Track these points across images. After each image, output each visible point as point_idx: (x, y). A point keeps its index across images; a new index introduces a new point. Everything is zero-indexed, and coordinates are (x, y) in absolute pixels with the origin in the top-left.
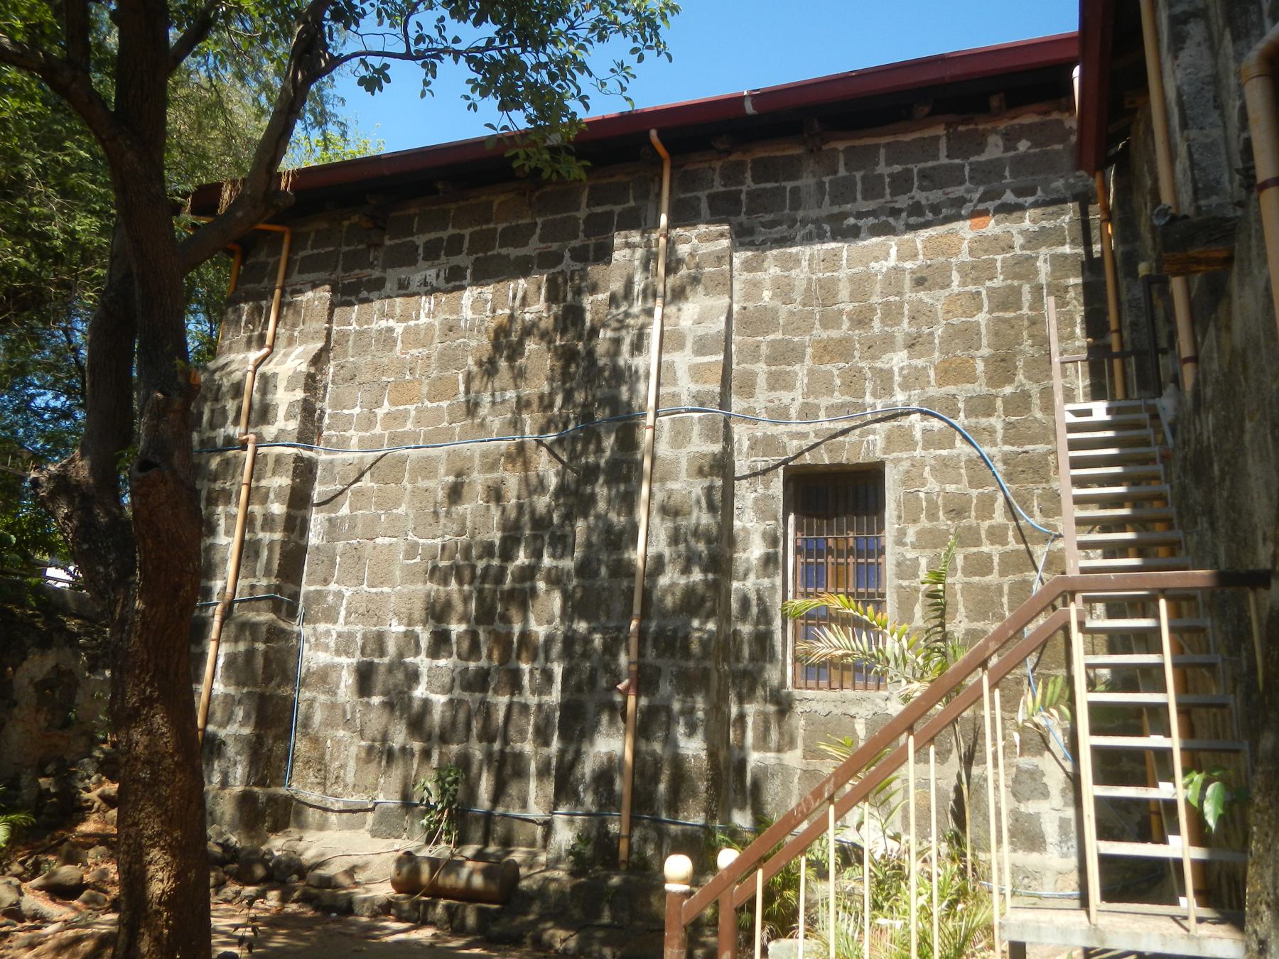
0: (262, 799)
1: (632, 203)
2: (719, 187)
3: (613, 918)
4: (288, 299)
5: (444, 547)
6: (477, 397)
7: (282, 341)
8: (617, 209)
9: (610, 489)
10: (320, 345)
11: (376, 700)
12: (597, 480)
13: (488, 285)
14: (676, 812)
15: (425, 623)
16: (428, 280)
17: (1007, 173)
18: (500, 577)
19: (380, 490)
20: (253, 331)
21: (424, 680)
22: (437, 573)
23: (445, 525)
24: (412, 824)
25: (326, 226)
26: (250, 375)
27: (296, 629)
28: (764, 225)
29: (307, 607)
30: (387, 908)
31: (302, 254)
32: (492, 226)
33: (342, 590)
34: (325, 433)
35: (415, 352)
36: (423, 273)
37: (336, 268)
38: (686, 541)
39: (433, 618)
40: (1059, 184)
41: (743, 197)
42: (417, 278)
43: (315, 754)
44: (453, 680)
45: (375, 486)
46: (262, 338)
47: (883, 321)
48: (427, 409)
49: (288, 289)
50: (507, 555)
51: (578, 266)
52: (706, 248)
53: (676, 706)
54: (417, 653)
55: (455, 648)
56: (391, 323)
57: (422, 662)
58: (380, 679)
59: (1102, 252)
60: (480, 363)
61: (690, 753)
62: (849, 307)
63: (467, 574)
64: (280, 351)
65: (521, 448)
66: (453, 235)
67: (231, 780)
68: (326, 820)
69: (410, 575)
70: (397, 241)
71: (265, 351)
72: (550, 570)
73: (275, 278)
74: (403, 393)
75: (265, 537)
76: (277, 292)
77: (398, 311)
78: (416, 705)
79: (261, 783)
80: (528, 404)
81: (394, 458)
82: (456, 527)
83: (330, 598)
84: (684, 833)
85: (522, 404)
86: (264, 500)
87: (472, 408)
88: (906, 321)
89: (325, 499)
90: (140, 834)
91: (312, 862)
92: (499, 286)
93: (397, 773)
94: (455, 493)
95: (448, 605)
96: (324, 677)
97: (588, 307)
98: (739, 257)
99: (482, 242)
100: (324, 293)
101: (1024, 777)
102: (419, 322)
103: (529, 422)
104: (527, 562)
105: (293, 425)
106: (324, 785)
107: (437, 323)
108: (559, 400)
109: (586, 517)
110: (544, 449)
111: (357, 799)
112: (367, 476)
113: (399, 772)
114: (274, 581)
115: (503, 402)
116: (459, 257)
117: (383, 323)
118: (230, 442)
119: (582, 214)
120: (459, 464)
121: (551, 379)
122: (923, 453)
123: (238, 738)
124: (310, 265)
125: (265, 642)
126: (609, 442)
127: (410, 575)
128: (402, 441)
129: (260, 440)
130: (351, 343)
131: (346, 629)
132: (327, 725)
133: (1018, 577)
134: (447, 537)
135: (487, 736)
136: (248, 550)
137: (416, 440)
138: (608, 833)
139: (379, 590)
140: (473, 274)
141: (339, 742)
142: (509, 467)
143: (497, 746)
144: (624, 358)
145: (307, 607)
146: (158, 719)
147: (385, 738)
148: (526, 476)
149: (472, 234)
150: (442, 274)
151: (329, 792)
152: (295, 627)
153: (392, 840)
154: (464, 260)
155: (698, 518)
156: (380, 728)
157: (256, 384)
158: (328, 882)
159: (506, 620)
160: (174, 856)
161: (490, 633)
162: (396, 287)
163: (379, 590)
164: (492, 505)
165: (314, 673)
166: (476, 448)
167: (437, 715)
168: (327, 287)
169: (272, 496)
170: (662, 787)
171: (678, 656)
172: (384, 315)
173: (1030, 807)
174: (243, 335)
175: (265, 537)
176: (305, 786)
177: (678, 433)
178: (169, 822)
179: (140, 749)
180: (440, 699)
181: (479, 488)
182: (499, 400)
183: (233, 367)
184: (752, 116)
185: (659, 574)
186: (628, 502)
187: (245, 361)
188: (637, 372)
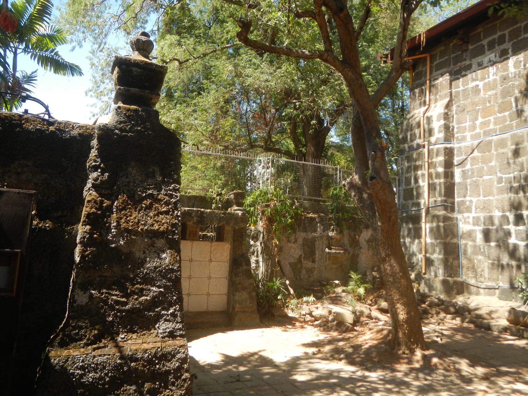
0: (451, 282)
4: (433, 83)
5: (514, 178)
6: (522, 107)
7: (433, 101)
10: (448, 99)
11: (493, 244)
13: (520, 53)
15: (510, 211)
16: (491, 59)
19: (482, 156)
20: (421, 100)
21: (513, 235)
22: (513, 190)
23: (514, 168)
24: (516, 296)
25: (443, 48)
26: (422, 118)
27: (455, 216)
29: (459, 207)
30: (505, 330)
31: (435, 63)
33: (472, 200)
34: (456, 136)
35: (489, 93)
36: (489, 57)
37: (450, 65)
43: (470, 265)
45: (480, 155)
46: (425, 102)
48: (499, 118)
49: (432, 79)
54: (509, 224)
56: (477, 83)
57: (512, 228)
58: (493, 235)
60: (521, 92)
64: (433, 105)
66: (500, 35)
67: (438, 275)
68: (479, 291)
69: (501, 191)
70: (475, 46)
71: (427, 107)
73: (426, 76)
74: (487, 112)
75: (437, 181)
76: (428, 82)
77: (479, 77)
78: (511, 247)
79: (450, 276)
81: (486, 141)
82: (519, 168)
83: (468, 203)
86: (435, 167)
90: (392, 299)
91: (474, 307)
93: (506, 274)
96: (470, 235)
99: (515, 34)
100: (447, 77)
102: (490, 79)
105: (442, 135)
106: (476, 278)
112: (476, 151)
114: (443, 198)
116: (505, 45)
117: (474, 84)
118: (419, 146)
120: (517, 140)
123: (438, 259)
124: (439, 67)
125: (443, 222)
127: (501, 191)
129: (430, 143)
130: (461, 95)
132: (474, 254)
134: (516, 173)
136: (432, 187)
137: (495, 132)
141: (479, 261)
145: (459, 207)
146: (392, 261)
147: (499, 260)
149: (509, 32)
150: (497, 55)
151: (479, 280)
152: (455, 215)
153: (508, 302)
154: (507, 45)
157: (425, 121)
158: (479, 317)
160: (405, 307)
162: (477, 66)
165: (465, 233)
168: (448, 74)
169: (437, 165)
172: (473, 80)
174: (418, 102)
175: (437, 181)
176: (468, 278)
178: (402, 295)
179: (388, 271)
183: (416, 116)
187: (419, 113)
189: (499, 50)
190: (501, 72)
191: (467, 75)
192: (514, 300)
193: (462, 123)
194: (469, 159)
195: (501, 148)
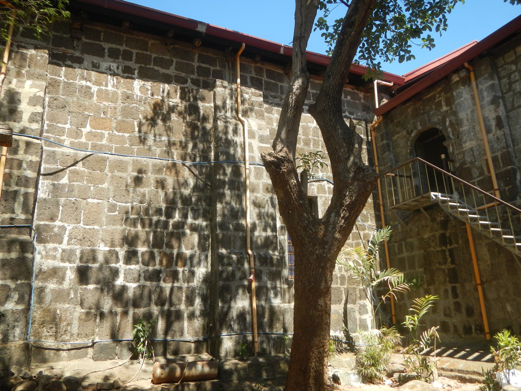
1: (218, 68)
2: (254, 75)
3: (267, 376)
8: (212, 68)
9: (231, 192)
11: (91, 287)
12: (225, 187)
14: (272, 329)
15: (122, 246)
17: (345, 105)
18: (166, 225)
21: (121, 276)
22: (129, 221)
23: (133, 197)
28: (272, 96)
32: (149, 53)
36: (109, 64)
38: (264, 218)
39: (126, 244)
40: (359, 114)
41: (263, 82)
42: (104, 65)
44: (140, 275)
45: (86, 170)
47: (313, 145)
49: (15, 44)
50: (169, 215)
51: (195, 87)
52: (254, 99)
53: (269, 286)
55: (140, 259)
57: (121, 265)
58: (93, 276)
59: (371, 140)
61: (276, 305)
62: (303, 137)
63: (147, 222)
65: (174, 165)
67: (11, 338)
69: (112, 221)
72: (192, 224)
78: (117, 289)
80: (174, 144)
83: (56, 230)
84: (278, 338)
85: (171, 144)
87: (143, 140)
88: (320, 147)
89: (50, 172)
92: (155, 84)
93: (107, 325)
94: (138, 181)
95: (136, 237)
97: (201, 108)
98: (266, 106)
101: (362, 307)
103: (175, 154)
104: (180, 220)
107: (119, 92)
108: (190, 146)
109: (221, 203)
110: (187, 169)
111: (79, 342)
112: (80, 164)
113: (108, 325)
115: (161, 141)
117: (84, 83)
119: (196, 64)
120: (139, 167)
121: (185, 135)
122: (329, 196)
126: (229, 170)
127: (112, 221)
128: (101, 149)
130: (61, 87)
131: (68, 247)
133: (356, 241)
135: (161, 302)
138: (247, 341)
139: (91, 227)
140: (139, 73)
142: (168, 173)
143: (166, 307)
144: (230, 136)
147: (98, 307)
148: (178, 179)
150: (120, 67)
155: (268, 209)
156: (94, 301)
159: (171, 247)
161: (160, 253)
162: (90, 65)
163: (91, 227)
164: (160, 190)
165: (45, 272)
166: (151, 162)
167: (130, 294)
168: (47, 51)
169: (24, 165)
170: (266, 320)
171: (269, 266)
172: (83, 78)
173: (364, 317)
177: (258, 174)
180: (132, 286)
181: (152, 181)
182: (158, 139)
184: (281, 55)
185: (254, 231)
186: (239, 198)
188: (236, 143)
189: (124, 65)
190: (124, 88)
191: (75, 68)
192: (117, 357)
193: (59, 123)
194: (68, 171)
195: (118, 171)
